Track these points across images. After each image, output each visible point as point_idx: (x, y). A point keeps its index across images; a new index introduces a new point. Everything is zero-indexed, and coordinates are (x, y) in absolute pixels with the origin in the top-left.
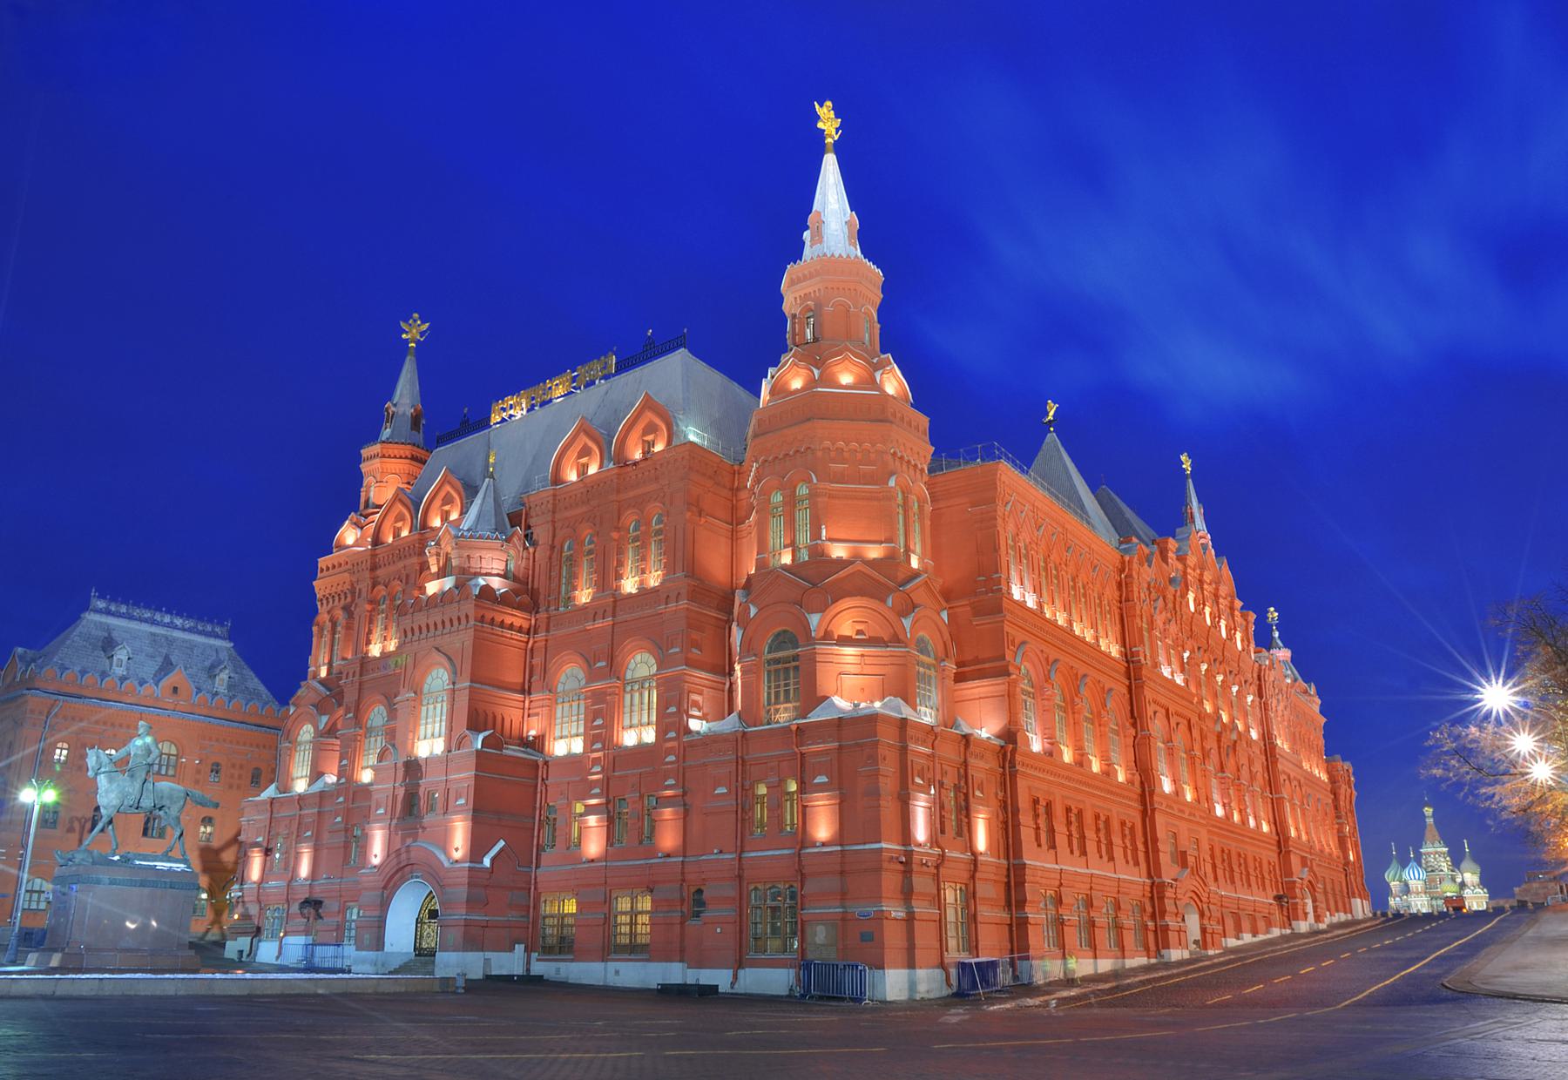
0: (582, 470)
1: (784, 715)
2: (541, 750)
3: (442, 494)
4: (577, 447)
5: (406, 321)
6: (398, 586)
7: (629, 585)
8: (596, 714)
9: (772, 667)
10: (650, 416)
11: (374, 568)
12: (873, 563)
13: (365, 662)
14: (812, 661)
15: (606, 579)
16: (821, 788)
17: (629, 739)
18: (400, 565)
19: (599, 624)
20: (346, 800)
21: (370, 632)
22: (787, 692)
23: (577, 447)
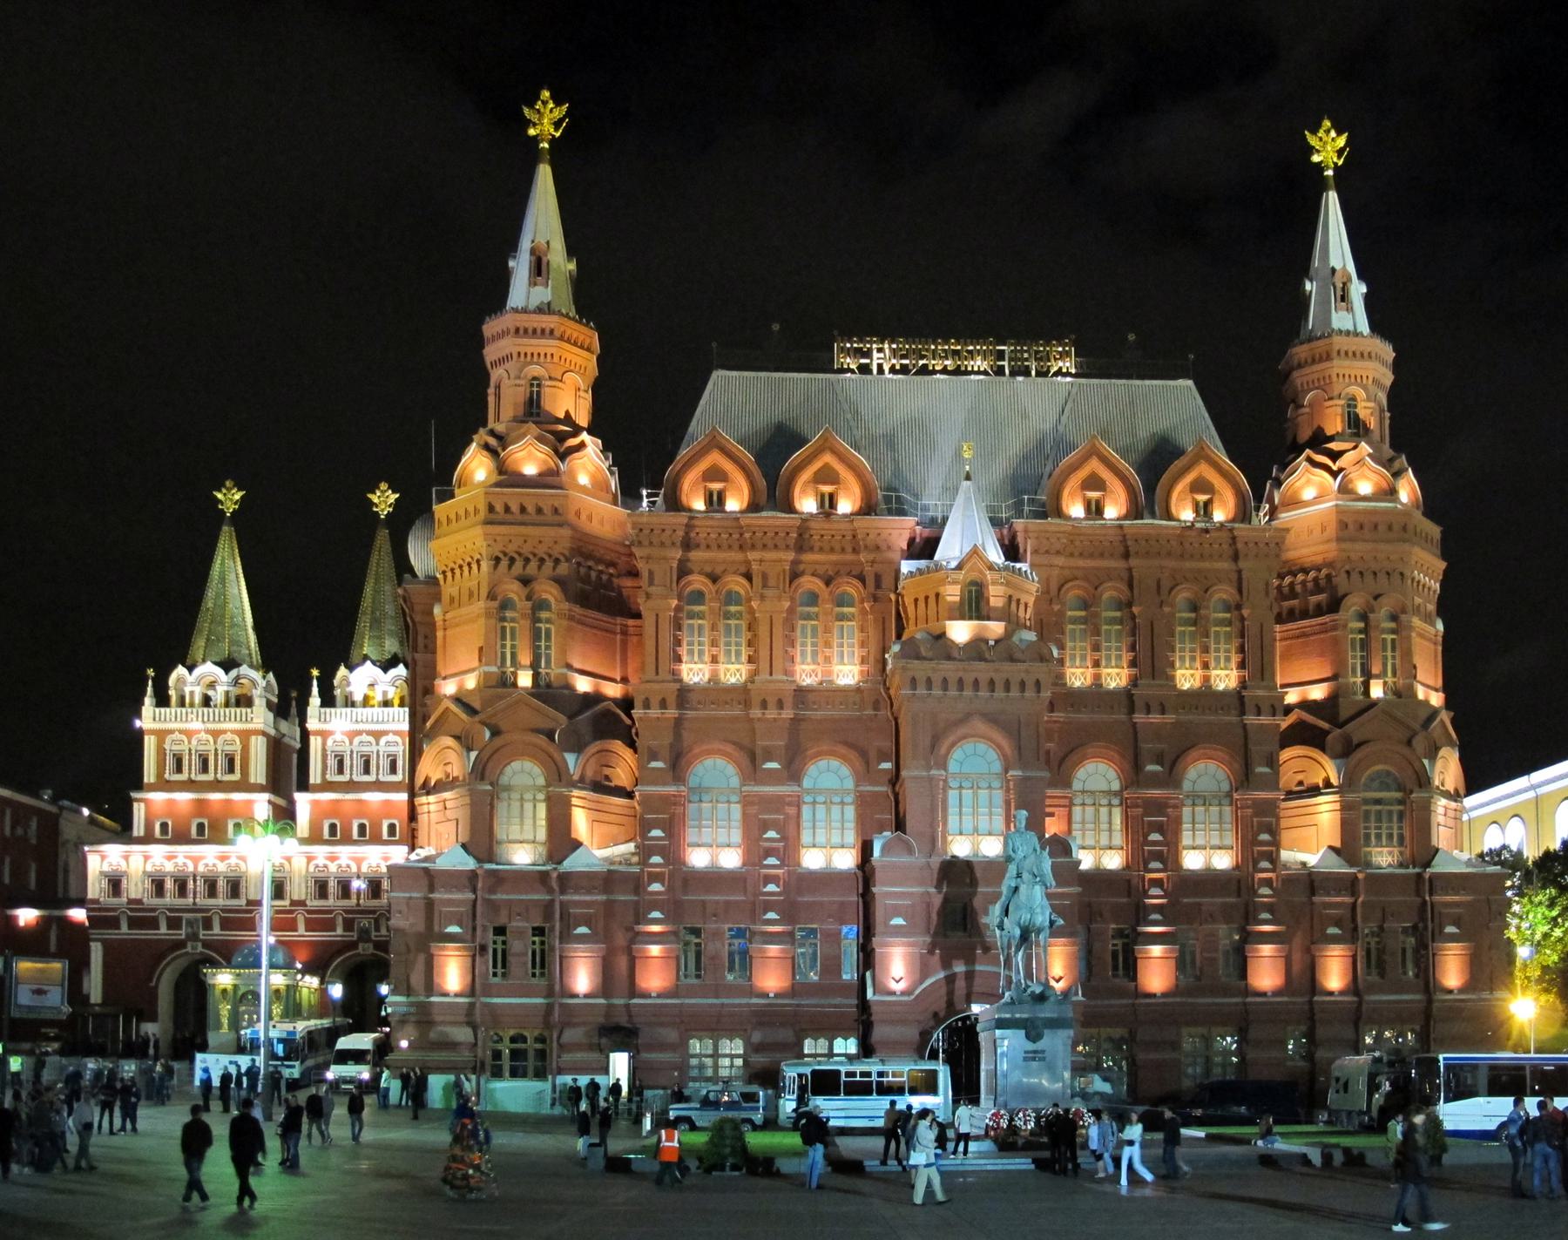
0: (1095, 510)
3: (817, 465)
4: (1083, 473)
5: (531, 106)
7: (1187, 678)
8: (1160, 828)
13: (684, 694)
15: (1151, 662)
16: (1453, 938)
17: (1192, 861)
18: (752, 555)
19: (1155, 718)
20: (670, 889)
21: (678, 643)
22: (1390, 836)
23: (1083, 473)
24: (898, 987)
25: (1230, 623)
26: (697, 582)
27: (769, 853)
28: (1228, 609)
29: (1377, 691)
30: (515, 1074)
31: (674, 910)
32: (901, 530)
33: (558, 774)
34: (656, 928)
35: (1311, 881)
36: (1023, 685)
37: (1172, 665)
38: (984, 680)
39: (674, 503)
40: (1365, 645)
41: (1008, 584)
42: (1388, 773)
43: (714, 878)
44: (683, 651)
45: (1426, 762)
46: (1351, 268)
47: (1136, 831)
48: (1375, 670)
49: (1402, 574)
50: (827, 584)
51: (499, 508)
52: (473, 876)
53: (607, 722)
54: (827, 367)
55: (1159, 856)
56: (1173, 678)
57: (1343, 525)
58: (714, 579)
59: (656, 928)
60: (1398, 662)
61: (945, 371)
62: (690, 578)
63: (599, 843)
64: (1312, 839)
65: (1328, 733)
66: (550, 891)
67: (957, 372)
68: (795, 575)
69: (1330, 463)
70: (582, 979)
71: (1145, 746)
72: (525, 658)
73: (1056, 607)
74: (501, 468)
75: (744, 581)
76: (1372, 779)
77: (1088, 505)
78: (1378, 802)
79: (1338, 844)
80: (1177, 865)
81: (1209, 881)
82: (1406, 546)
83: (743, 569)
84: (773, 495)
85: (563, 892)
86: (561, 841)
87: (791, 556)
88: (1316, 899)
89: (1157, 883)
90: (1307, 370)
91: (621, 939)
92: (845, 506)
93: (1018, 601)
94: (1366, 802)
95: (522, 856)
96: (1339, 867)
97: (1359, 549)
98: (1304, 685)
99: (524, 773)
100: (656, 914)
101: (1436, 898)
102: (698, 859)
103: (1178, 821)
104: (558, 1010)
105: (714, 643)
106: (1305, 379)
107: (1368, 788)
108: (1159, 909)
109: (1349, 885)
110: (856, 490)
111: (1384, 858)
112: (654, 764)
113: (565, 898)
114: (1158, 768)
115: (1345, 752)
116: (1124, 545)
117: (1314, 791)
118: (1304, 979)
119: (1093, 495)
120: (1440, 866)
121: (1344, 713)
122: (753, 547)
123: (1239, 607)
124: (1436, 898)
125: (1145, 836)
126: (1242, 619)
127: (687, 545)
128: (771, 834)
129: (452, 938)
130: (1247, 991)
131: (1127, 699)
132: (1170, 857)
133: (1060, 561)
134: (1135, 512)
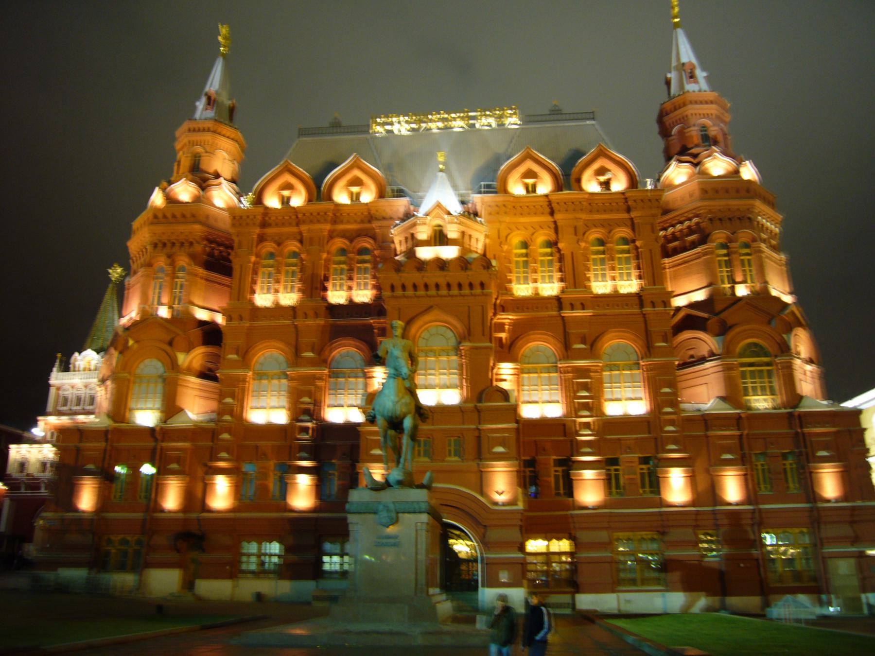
4: (522, 169)
6: (293, 246)
8: (585, 387)
15: (574, 276)
18: (304, 228)
19: (579, 313)
21: (254, 282)
25: (628, 252)
28: (625, 241)
32: (401, 204)
34: (222, 464)
35: (706, 420)
37: (588, 279)
40: (729, 264)
42: (756, 345)
44: (258, 288)
45: (785, 336)
46: (694, 61)
47: (570, 391)
48: (739, 278)
49: (749, 218)
50: (351, 241)
52: (105, 434)
53: (211, 334)
55: (586, 406)
56: (589, 287)
57: (704, 191)
59: (222, 464)
60: (754, 273)
62: (265, 244)
64: (704, 394)
65: (706, 320)
66: (156, 440)
68: (331, 237)
69: (692, 160)
71: (572, 331)
72: (165, 299)
73: (505, 247)
75: (298, 244)
77: (526, 186)
78: (751, 365)
79: (723, 394)
80: (603, 414)
81: (626, 423)
82: (751, 202)
83: (299, 237)
84: (319, 191)
85: (162, 441)
86: (171, 408)
87: (328, 227)
88: (711, 433)
89: (587, 425)
90: (672, 115)
93: (470, 236)
94: (743, 365)
97: (718, 204)
98: (689, 293)
99: (152, 366)
100: (224, 455)
101: (806, 430)
103: (600, 382)
106: (670, 121)
107: (741, 356)
108: (588, 443)
109: (737, 421)
110: (373, 187)
111: (761, 403)
113: (164, 444)
114: (582, 346)
115: (723, 330)
117: (703, 360)
118: (707, 492)
119: (530, 181)
121: (719, 307)
122: (304, 222)
123: (634, 241)
124: (806, 430)
125: (575, 392)
126: (637, 248)
127: (264, 225)
130: (662, 503)
131: (558, 301)
132: (595, 408)
134: (559, 186)
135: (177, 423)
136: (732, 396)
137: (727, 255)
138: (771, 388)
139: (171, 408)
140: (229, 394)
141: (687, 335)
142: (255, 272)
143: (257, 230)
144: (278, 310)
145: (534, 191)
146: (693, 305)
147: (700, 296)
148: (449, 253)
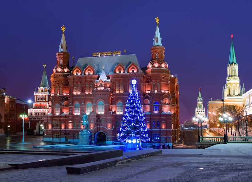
1: (156, 112)
2: (115, 113)
3: (88, 69)
4: (118, 68)
6: (79, 83)
9: (154, 106)
10: (133, 66)
11: (74, 79)
12: (167, 93)
13: (74, 96)
14: (161, 106)
16: (163, 122)
21: (73, 90)
23: (118, 68)
24: (109, 128)
26: (75, 83)
27: (82, 113)
29: (156, 92)
30: (56, 137)
31: (72, 120)
33: (61, 105)
36: (106, 94)
38: (101, 94)
39: (73, 75)
41: (104, 83)
43: (77, 116)
51: (55, 76)
54: (92, 56)
57: (152, 71)
58: (77, 83)
61: (105, 56)
63: (66, 112)
67: (107, 56)
70: (63, 127)
74: (56, 71)
76: (154, 103)
78: (155, 105)
86: (61, 112)
91: (67, 123)
92: (91, 73)
95: (58, 114)
96: (149, 114)
99: (58, 105)
100: (70, 120)
102: (75, 114)
104: (61, 131)
105: (77, 90)
107: (154, 104)
112: (70, 104)
116: (123, 76)
117: (148, 104)
120: (162, 113)
128: (83, 111)
129: (50, 123)
133: (115, 78)
135: (62, 115)
136: (151, 111)
137: (155, 84)
138: (158, 110)
139: (61, 112)
140: (71, 110)
141: (146, 99)
142: (73, 88)
143: (72, 80)
144: (77, 95)
145: (121, 72)
146: (148, 94)
147: (149, 92)
148: (102, 88)
